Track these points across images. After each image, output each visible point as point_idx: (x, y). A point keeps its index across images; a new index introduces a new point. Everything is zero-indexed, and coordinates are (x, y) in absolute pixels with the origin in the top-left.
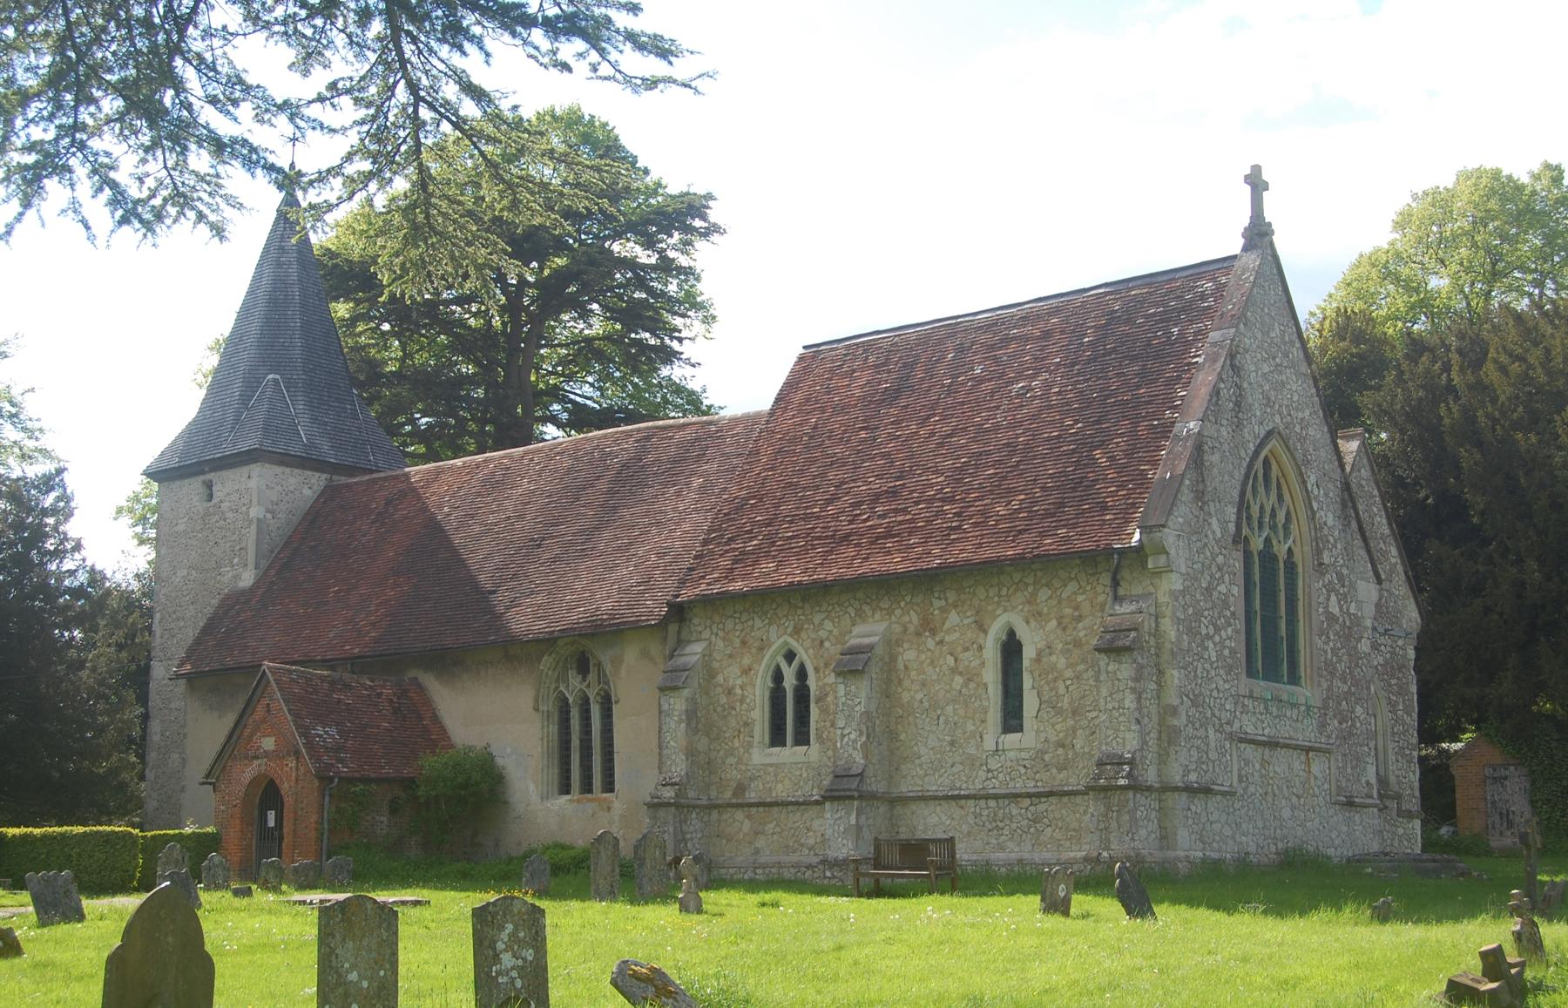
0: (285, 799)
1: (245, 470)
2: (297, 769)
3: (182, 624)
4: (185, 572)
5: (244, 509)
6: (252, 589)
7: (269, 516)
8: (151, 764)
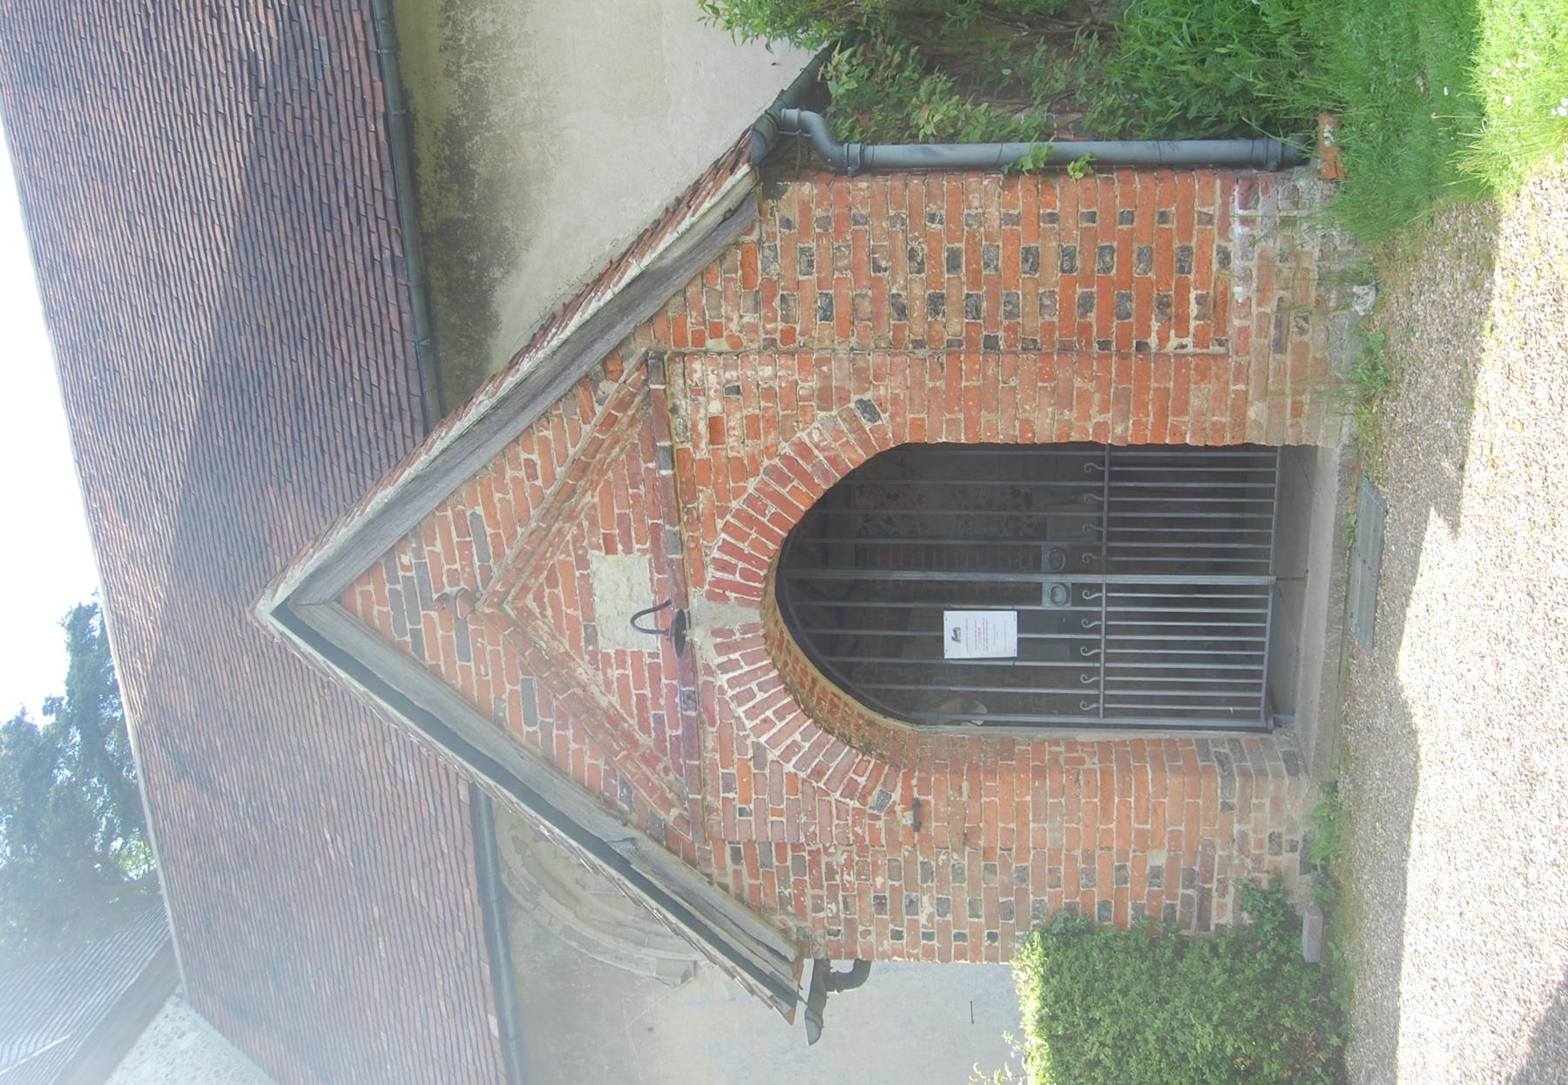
0: (889, 431)
2: (737, 351)
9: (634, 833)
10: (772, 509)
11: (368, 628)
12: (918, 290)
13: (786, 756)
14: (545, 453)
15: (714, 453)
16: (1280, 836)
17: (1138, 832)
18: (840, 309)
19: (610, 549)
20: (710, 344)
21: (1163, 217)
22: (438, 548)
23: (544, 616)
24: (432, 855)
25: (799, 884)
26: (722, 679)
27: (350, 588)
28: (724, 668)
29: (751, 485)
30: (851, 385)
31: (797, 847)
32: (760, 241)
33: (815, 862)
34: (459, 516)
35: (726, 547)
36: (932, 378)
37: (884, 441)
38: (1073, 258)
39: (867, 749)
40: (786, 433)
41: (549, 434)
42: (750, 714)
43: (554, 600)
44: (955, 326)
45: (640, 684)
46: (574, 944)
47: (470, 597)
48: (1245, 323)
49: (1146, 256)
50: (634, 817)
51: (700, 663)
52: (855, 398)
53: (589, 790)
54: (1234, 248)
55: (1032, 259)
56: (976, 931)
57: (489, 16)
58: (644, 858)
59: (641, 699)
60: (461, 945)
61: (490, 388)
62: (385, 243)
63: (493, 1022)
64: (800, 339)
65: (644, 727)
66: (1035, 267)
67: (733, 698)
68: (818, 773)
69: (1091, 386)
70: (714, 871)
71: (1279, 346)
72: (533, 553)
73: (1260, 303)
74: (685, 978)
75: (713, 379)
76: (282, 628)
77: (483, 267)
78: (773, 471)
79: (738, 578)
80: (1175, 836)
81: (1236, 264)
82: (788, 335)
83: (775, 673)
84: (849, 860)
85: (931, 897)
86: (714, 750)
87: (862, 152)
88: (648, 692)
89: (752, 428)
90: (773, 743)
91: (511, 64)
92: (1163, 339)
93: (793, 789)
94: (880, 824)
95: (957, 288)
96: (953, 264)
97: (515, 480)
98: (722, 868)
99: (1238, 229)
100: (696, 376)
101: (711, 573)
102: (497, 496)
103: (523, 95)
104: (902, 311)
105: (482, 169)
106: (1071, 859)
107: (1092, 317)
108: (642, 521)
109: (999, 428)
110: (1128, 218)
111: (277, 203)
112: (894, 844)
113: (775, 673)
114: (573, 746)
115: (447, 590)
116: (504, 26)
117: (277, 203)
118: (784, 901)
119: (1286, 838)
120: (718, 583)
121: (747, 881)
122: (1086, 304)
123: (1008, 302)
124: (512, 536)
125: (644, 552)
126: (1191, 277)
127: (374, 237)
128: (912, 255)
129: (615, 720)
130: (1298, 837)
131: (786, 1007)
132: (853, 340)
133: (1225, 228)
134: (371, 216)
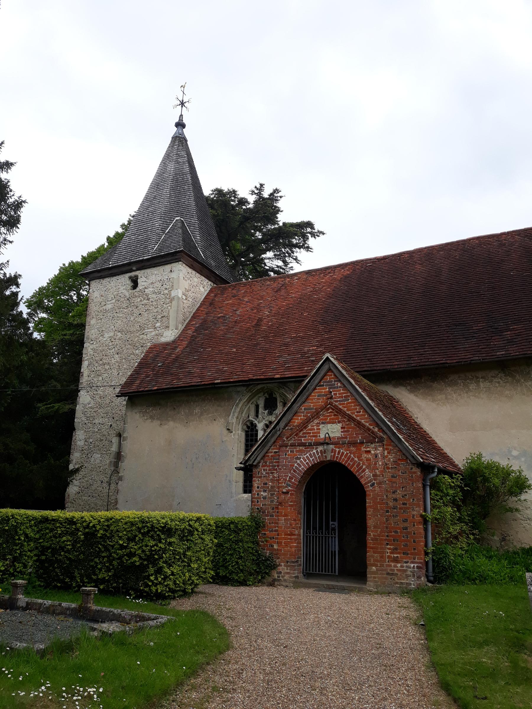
0: (369, 489)
1: (168, 267)
2: (384, 457)
3: (107, 367)
4: (112, 334)
5: (166, 292)
6: (174, 342)
7: (184, 297)
8: (74, 461)
9: (281, 431)
10: (351, 463)
11: (325, 375)
12: (398, 496)
13: (298, 464)
14: (362, 415)
15: (363, 451)
16: (281, 574)
17: (282, 542)
18: (394, 479)
19: (342, 428)
20: (386, 452)
21: (414, 549)
22: (342, 391)
23: (328, 413)
24: (260, 366)
25: (269, 466)
26: (315, 451)
27: (332, 372)
28: (317, 451)
29: (356, 459)
30: (378, 481)
31: (278, 466)
32: (408, 463)
33: (275, 470)
34: (348, 396)
35: (343, 453)
36: (380, 499)
37: (367, 487)
38: (406, 529)
39: (299, 482)
40: (367, 467)
41: (366, 416)
42: (307, 457)
43: (331, 416)
44: (391, 504)
45: (313, 433)
46: (237, 401)
47: (331, 398)
48: (393, 566)
49: (406, 545)
50: (284, 431)
51: (318, 447)
52: (375, 482)
53: (290, 421)
54: (408, 564)
55: (405, 521)
56: (259, 505)
57: (474, 387)
58: (276, 432)
59: (310, 433)
60: (238, 373)
61: (376, 405)
62: (415, 362)
63: (219, 381)
64: (387, 471)
65: (304, 433)
66: (404, 521)
67: (311, 453)
68: (294, 471)
69: (379, 533)
70: (272, 447)
71: (388, 574)
72: (341, 412)
73: (397, 570)
74: (228, 429)
75: (378, 452)
76: (324, 358)
77: (410, 384)
78: (359, 464)
79: (336, 455)
80: (281, 550)
81: (405, 565)
82: (388, 468)
83: (316, 462)
84: (275, 477)
85: (267, 495)
86: (299, 449)
87: (428, 485)
88: (311, 435)
89: (368, 460)
90: (301, 462)
91: (462, 393)
92: (389, 549)
93: (291, 466)
94: (283, 484)
95: (399, 505)
96: (404, 504)
97: (356, 409)
98: (273, 449)
99: (412, 565)
100: (379, 448)
101: (337, 450)
102: (353, 405)
103: (454, 396)
104: (394, 492)
105: (435, 385)
106: (275, 527)
107: (393, 533)
108: (348, 435)
109: (370, 512)
110: (414, 542)
111: (426, 331)
112: (279, 487)
113: (316, 462)
114: (299, 418)
115: (333, 393)
116: (472, 391)
117: (426, 331)
118: (266, 462)
119: (281, 575)
120: (335, 451)
121: (270, 454)
122: (396, 532)
123: (396, 515)
124: (344, 407)
125: (341, 435)
126: (402, 555)
127: (417, 358)
128: (406, 495)
129: (305, 428)
130: (281, 578)
131: (243, 462)
132: (387, 482)
133: (412, 563)
134: (422, 358)
